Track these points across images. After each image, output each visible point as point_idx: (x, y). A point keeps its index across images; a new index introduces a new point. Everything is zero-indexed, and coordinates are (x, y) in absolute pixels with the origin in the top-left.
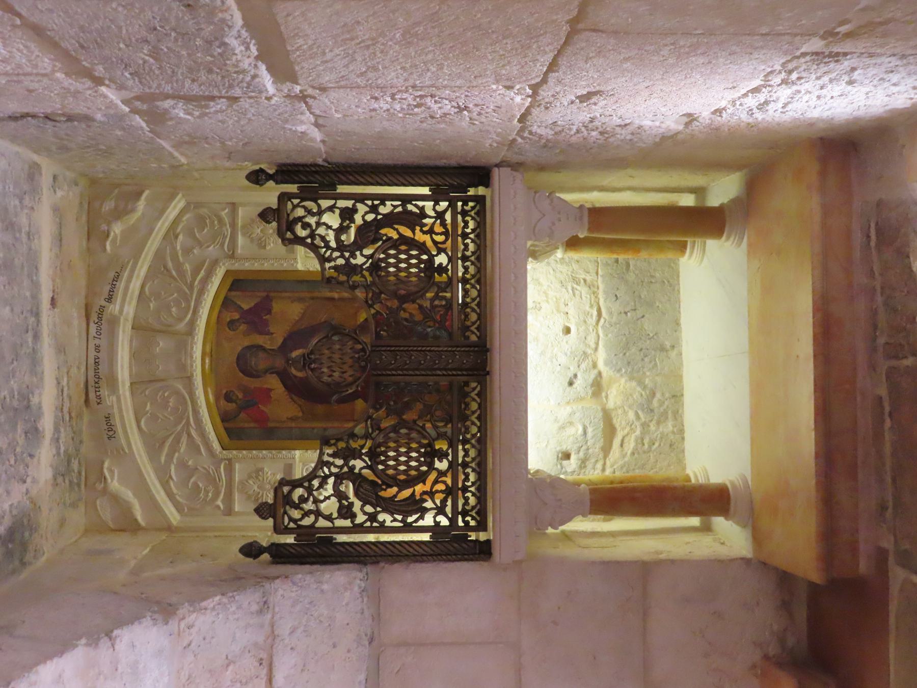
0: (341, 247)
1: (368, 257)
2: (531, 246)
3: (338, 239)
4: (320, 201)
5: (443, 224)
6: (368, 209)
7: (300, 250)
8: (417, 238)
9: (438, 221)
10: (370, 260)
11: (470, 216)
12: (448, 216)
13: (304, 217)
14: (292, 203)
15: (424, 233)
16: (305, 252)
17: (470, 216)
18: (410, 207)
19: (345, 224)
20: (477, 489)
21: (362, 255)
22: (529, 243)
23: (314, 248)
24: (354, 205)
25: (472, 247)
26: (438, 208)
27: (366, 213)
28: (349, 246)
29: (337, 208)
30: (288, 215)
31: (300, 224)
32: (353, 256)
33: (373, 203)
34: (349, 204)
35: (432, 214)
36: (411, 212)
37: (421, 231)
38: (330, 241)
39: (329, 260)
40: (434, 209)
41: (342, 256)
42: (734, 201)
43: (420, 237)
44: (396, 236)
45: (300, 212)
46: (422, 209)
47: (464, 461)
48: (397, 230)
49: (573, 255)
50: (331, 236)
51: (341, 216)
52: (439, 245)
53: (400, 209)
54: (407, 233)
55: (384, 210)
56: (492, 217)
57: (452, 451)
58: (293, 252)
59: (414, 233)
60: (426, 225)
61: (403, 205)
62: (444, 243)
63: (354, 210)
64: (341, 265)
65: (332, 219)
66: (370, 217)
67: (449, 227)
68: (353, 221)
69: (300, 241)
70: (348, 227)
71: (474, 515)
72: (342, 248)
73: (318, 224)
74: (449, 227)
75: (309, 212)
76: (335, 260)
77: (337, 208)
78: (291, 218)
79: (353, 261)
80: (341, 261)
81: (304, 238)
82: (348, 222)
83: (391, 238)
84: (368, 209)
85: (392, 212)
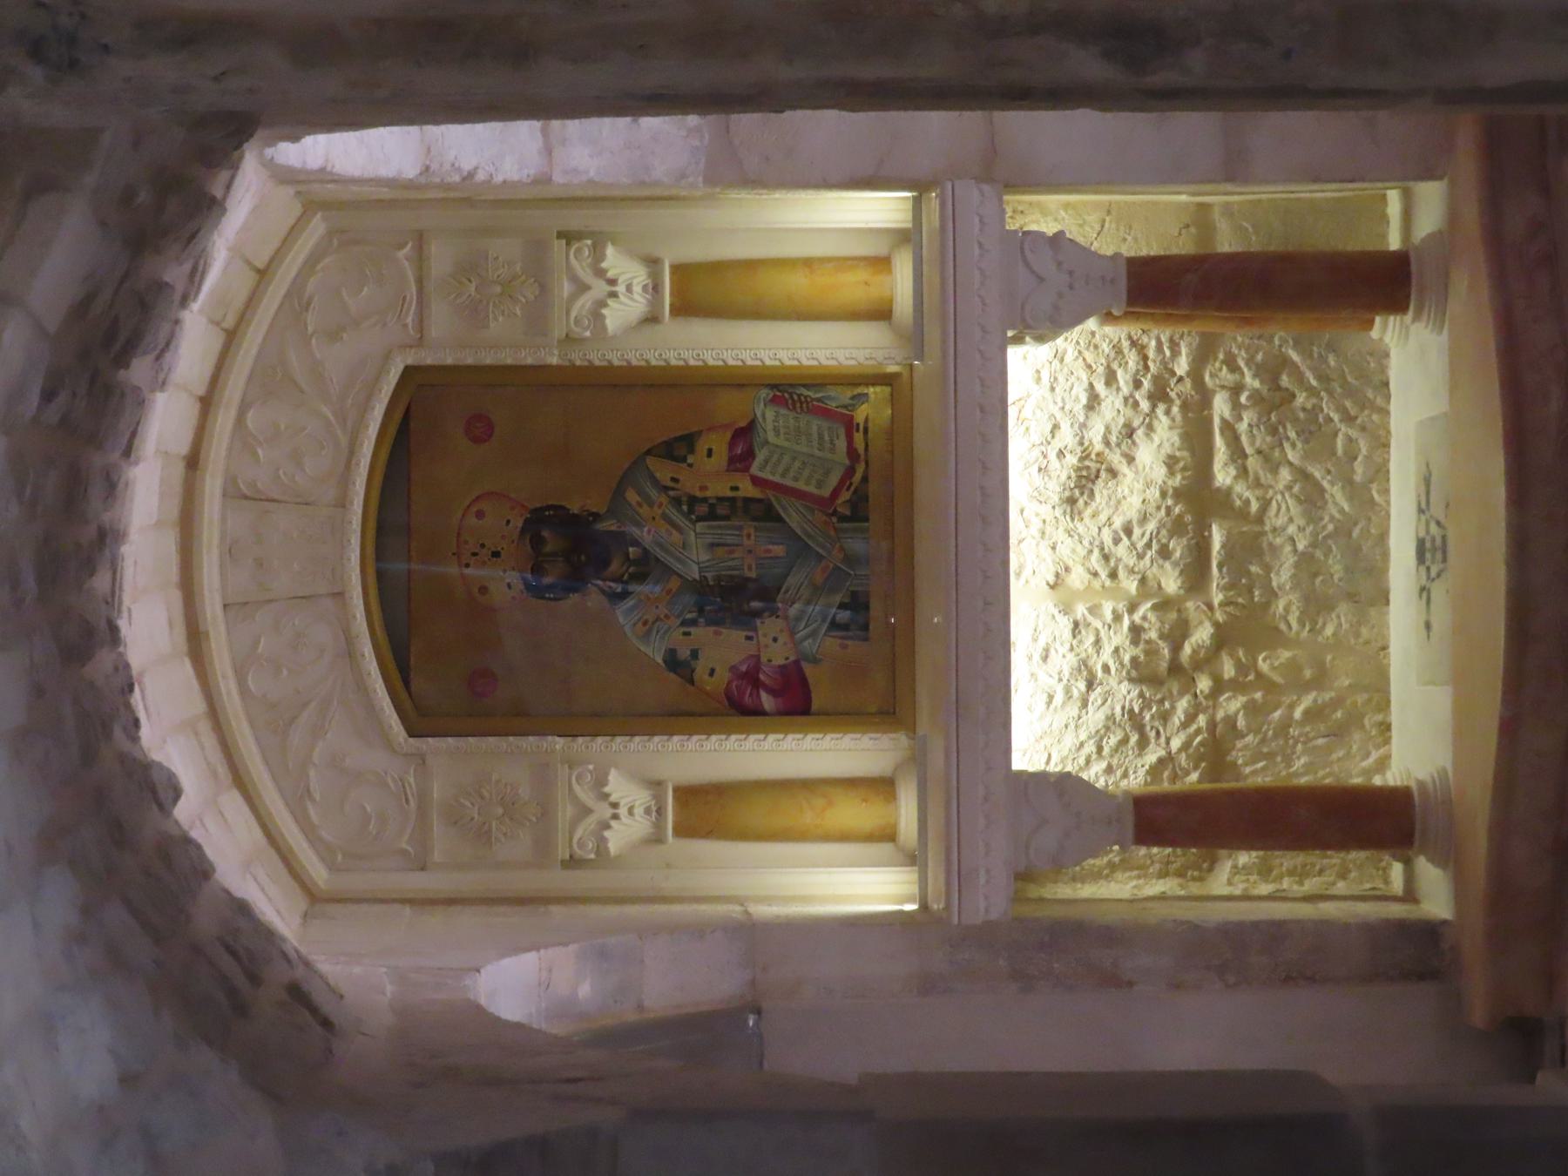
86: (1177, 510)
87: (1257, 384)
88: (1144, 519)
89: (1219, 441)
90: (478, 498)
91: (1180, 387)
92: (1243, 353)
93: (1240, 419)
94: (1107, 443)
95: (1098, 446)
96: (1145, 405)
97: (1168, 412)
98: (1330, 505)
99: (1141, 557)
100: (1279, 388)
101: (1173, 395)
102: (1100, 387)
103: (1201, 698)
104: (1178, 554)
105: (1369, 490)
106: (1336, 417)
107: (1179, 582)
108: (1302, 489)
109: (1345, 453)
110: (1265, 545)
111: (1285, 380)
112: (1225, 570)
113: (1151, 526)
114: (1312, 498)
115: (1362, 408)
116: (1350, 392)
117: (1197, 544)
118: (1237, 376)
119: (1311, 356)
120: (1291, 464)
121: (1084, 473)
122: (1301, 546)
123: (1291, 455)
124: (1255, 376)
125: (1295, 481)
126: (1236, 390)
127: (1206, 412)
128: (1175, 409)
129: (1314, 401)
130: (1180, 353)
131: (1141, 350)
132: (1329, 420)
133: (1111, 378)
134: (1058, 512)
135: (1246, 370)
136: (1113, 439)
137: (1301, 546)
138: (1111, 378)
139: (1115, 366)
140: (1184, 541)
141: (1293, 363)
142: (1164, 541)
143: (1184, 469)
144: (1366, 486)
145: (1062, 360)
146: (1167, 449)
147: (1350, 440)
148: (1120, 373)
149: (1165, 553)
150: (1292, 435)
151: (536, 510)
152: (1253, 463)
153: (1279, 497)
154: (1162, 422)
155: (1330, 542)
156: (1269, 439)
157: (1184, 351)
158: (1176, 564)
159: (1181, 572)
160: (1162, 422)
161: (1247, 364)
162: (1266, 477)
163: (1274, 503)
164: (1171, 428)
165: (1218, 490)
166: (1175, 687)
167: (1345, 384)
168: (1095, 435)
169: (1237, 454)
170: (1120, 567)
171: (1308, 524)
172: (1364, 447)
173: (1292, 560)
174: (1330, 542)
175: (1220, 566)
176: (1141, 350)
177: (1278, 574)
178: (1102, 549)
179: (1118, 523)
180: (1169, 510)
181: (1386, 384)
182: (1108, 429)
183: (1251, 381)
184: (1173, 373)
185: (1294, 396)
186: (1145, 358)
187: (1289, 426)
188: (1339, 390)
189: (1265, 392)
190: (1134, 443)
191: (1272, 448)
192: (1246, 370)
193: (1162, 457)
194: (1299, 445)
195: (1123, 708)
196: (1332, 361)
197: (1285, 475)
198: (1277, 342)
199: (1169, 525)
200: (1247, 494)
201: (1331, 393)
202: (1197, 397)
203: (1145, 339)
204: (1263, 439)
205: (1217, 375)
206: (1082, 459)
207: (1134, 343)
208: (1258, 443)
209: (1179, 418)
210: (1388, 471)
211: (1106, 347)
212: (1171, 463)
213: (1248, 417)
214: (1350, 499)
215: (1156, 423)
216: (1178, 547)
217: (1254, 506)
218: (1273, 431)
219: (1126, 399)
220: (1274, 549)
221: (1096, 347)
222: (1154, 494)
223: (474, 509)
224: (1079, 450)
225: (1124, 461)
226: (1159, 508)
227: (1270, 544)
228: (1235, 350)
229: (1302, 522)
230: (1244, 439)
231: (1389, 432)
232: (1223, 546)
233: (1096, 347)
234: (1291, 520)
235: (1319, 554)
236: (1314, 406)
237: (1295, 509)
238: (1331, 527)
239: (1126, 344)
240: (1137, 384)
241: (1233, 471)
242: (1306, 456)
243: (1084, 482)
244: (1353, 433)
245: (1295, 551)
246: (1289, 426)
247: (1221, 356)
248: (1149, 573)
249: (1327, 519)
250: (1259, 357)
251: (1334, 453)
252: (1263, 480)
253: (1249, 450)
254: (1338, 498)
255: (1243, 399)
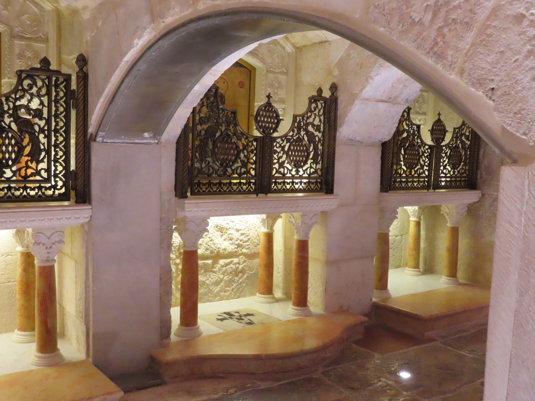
0: (16, 108)
1: (9, 126)
2: (28, 231)
3: (21, 106)
4: (46, 97)
5: (32, 175)
6: (42, 126)
7: (14, 81)
8: (23, 157)
9: (34, 171)
10: (7, 127)
11: (38, 192)
12: (38, 178)
13: (36, 86)
14: (46, 79)
15: (26, 162)
16: (14, 84)
17: (38, 192)
18: (43, 154)
19: (32, 112)
20: (9, 197)
21: (11, 122)
22: (30, 230)
23: (15, 91)
24: (45, 118)
25: (17, 193)
26: (319, 170)
27: (39, 126)
28: (17, 114)
29: (43, 108)
30: (38, 76)
31: (32, 83)
32: (10, 116)
33: (46, 130)
34: (45, 115)
35: (39, 168)
36: (40, 154)
37: (28, 160)
38: (20, 101)
39: (7, 100)
40: (42, 169)
41: (9, 109)
42: (61, 356)
43: (24, 159)
44: (24, 144)
45: (40, 83)
46: (42, 161)
47: (28, 187)
48: (28, 144)
49: (18, 260)
50: (24, 102)
51: (37, 110)
52: (18, 173)
53: (42, 147)
54: (27, 150)
55: (41, 136)
56: (32, 207)
57: (298, 177)
58: (15, 77)
59: (26, 156)
60: (32, 163)
61: (44, 149)
62: (20, 175)
63: (41, 119)
64: (3, 108)
65: (35, 104)
66: (37, 128)
67: (31, 178)
68: (34, 117)
69: (20, 81)
70: (30, 114)
71: (8, 195)
72: (15, 109)
73: (32, 95)
74: (31, 178)
75: (40, 89)
76: (7, 104)
77: (43, 108)
78: (35, 77)
79: (6, 116)
80: (6, 108)
81: (22, 85)
82: (33, 114)
83: (23, 141)
84: (42, 127)
85: (40, 142)
86: (215, 252)
87: (240, 268)
88: (214, 244)
89: (229, 260)
90: (228, 83)
91: (240, 250)
92: (246, 264)
93: (233, 265)
94: (229, 234)
95: (228, 232)
96: (237, 243)
97: (235, 248)
98: (215, 288)
99: (206, 244)
100: (239, 273)
101: (238, 249)
102: (240, 232)
103: (175, 261)
104: (206, 252)
105: (218, 296)
106: (233, 287)
107: (201, 253)
108: (219, 281)
109: (226, 290)
110: (207, 273)
111: (241, 274)
112: (203, 264)
113: (213, 246)
114: (217, 283)
115: (235, 293)
116: (238, 289)
117: (208, 257)
118: (242, 263)
119: (245, 280)
120: (224, 278)
121: (223, 229)
122: (207, 282)
123: (226, 277)
124: (242, 267)
125: (220, 279)
126: (239, 263)
127: (234, 257)
128: (236, 250)
129: (236, 281)
130: (247, 250)
131: (247, 241)
132: (232, 285)
133: (242, 234)
134: (216, 224)
135: (243, 265)
136: (230, 236)
137: (207, 282)
138: (242, 234)
139: (245, 235)
140: (209, 254)
141: (244, 276)
142: (209, 249)
143: (223, 253)
144: (220, 296)
145: (246, 223)
146: (228, 248)
147: (228, 291)
148: (243, 236)
149: (207, 249)
150: (230, 277)
151: (224, 97)
152: (224, 268)
153: (217, 276)
154: (233, 247)
155: (208, 288)
156: (229, 272)
157: (247, 251)
158: (204, 252)
159: (203, 254)
160: (233, 247)
161: (244, 265)
162: (221, 272)
163: (215, 274)
164: (232, 249)
165: (218, 261)
166: (177, 254)
167: (239, 288)
168: (231, 231)
169: (227, 265)
170: (204, 239)
171: (212, 283)
172: (227, 294)
173: (204, 280)
174: (208, 288)
175: (203, 263)
176: (247, 241)
177: (201, 277)
178: (208, 234)
179: (213, 238)
180: (215, 250)
181: (239, 298)
182: (232, 234)
183: (241, 267)
184: (242, 249)
185: (237, 276)
186: (246, 242)
187: (232, 276)
188: (238, 287)
189: (238, 270)
190: (229, 240)
191: (227, 273)
192: (243, 265)
193: (226, 247)
194: (228, 279)
195: (174, 242)
196: (244, 285)
197: (222, 276)
198: (248, 272)
199: (213, 250)
200: (217, 268)
201: (238, 285)
202: (238, 254)
203: (250, 242)
204: (229, 270)
205: (242, 259)
206: (226, 229)
207: (249, 239)
208: (228, 269)
209: (234, 251)
210: (222, 300)
211: (248, 233)
212: (225, 249)
213: (234, 267)
214: (217, 292)
215: (233, 245)
216: (208, 252)
217: (215, 270)
218: (231, 273)
219: (238, 238)
220: (206, 275)
221: (248, 231)
222: (219, 246)
223: (225, 82)
224: (228, 228)
225: (225, 238)
226: (216, 247)
227: (207, 274)
228: (247, 262)
229: (212, 281)
230: (229, 266)
231: (229, 299)
232: (208, 263)
233: (248, 231)
234: (212, 279)
235: (205, 286)
236: (235, 282)
237: (214, 279)
238: (211, 288)
239: (249, 237)
240: (241, 241)
241: (223, 264)
242: (226, 281)
243: (221, 229)
244: (230, 291)
245: (206, 280)
246: (232, 276)
247: (246, 259)
248: (202, 246)
249: (213, 287)
250: (245, 268)
251: (226, 287)
252: (220, 271)
253: (227, 267)
254: (217, 289)
255: (237, 265)
